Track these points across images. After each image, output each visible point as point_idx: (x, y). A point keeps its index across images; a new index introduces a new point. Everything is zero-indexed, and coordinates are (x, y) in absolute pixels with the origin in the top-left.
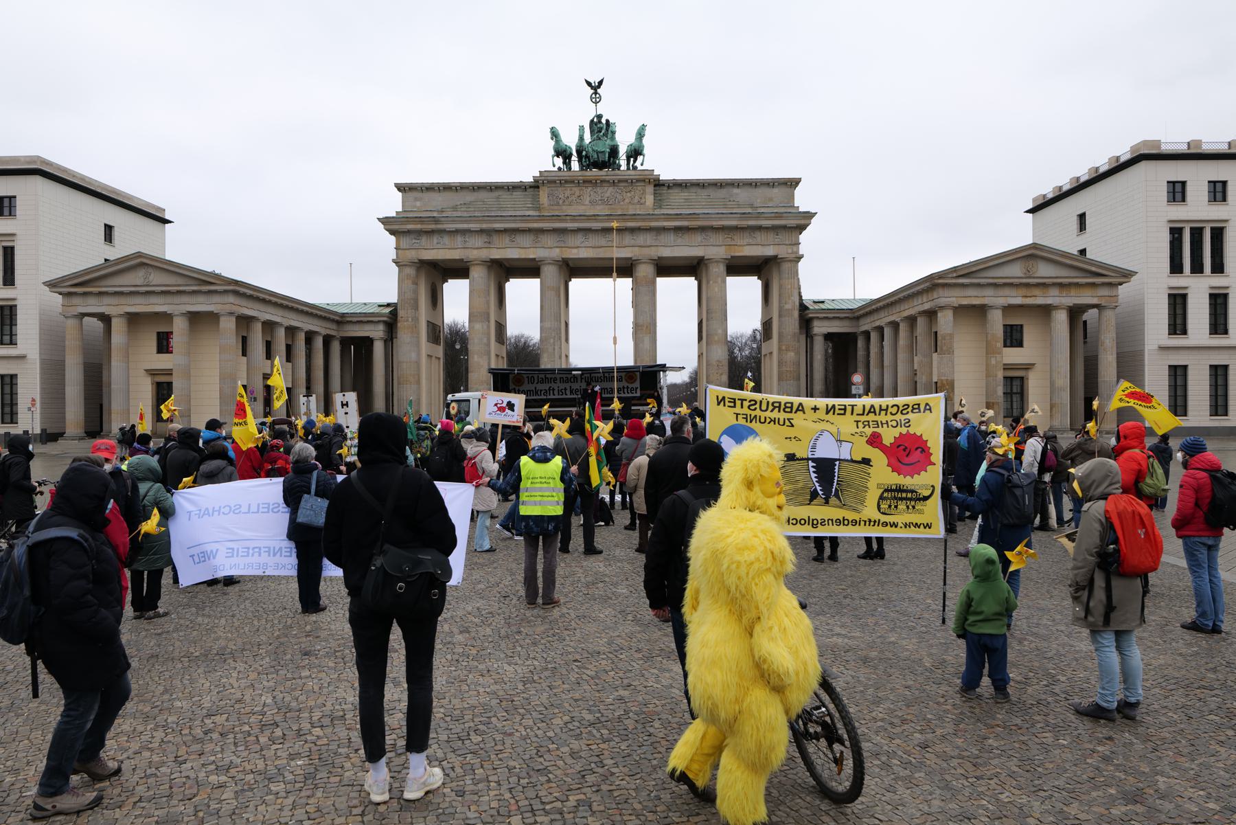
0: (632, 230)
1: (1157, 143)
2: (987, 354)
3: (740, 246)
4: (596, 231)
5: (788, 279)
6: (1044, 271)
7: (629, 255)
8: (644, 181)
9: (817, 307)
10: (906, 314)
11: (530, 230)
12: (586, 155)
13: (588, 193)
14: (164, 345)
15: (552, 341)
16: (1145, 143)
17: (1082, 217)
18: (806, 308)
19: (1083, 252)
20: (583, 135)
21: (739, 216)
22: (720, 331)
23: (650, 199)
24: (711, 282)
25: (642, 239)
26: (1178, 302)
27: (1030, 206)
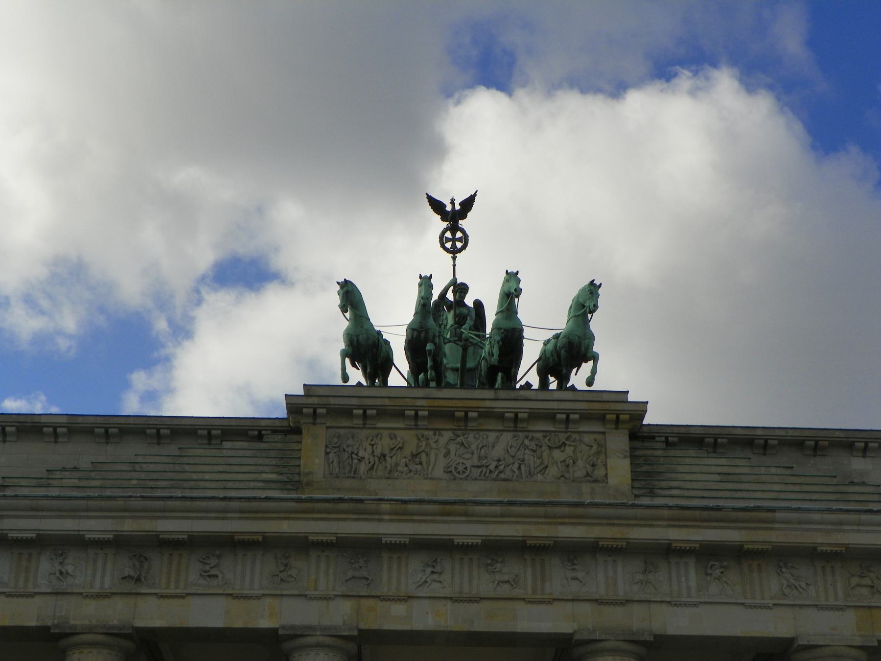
4: (466, 549)
7: (564, 627)
8: (601, 418)
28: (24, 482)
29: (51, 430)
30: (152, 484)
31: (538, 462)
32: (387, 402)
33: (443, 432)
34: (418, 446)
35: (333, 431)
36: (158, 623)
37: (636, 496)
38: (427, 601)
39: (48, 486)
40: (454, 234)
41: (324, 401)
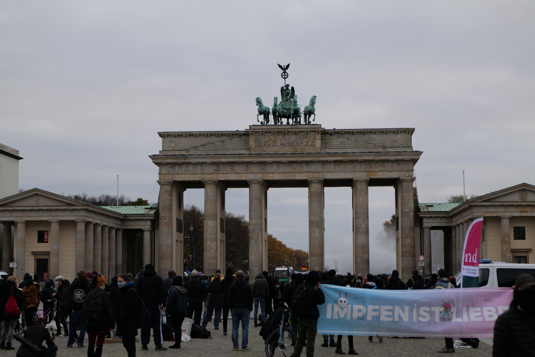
0: (307, 162)
2: (502, 244)
3: (376, 172)
4: (285, 163)
5: (407, 192)
8: (315, 131)
9: (426, 210)
11: (243, 163)
12: (278, 115)
13: (280, 140)
14: (42, 238)
15: (257, 232)
18: (419, 210)
20: (277, 103)
21: (374, 154)
22: (363, 226)
23: (318, 143)
24: (358, 195)
28: (192, 150)
29: (196, 135)
30: (218, 149)
31: (301, 142)
32: (267, 130)
33: (280, 136)
34: (275, 139)
35: (256, 136)
36: (223, 179)
37: (322, 149)
38: (277, 174)
39: (197, 150)
40: (285, 74)
41: (253, 130)
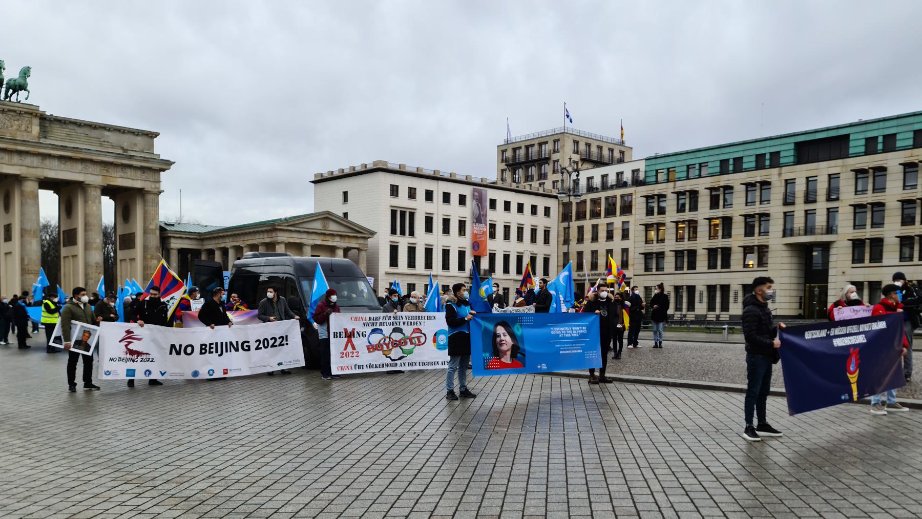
0: (20, 153)
1: (386, 163)
3: (116, 177)
5: (152, 206)
6: (333, 227)
8: (31, 114)
10: (250, 243)
16: (380, 162)
17: (345, 194)
19: (346, 214)
21: (115, 155)
23: (36, 129)
24: (90, 202)
25: (29, 160)
26: (394, 250)
27: (313, 180)
